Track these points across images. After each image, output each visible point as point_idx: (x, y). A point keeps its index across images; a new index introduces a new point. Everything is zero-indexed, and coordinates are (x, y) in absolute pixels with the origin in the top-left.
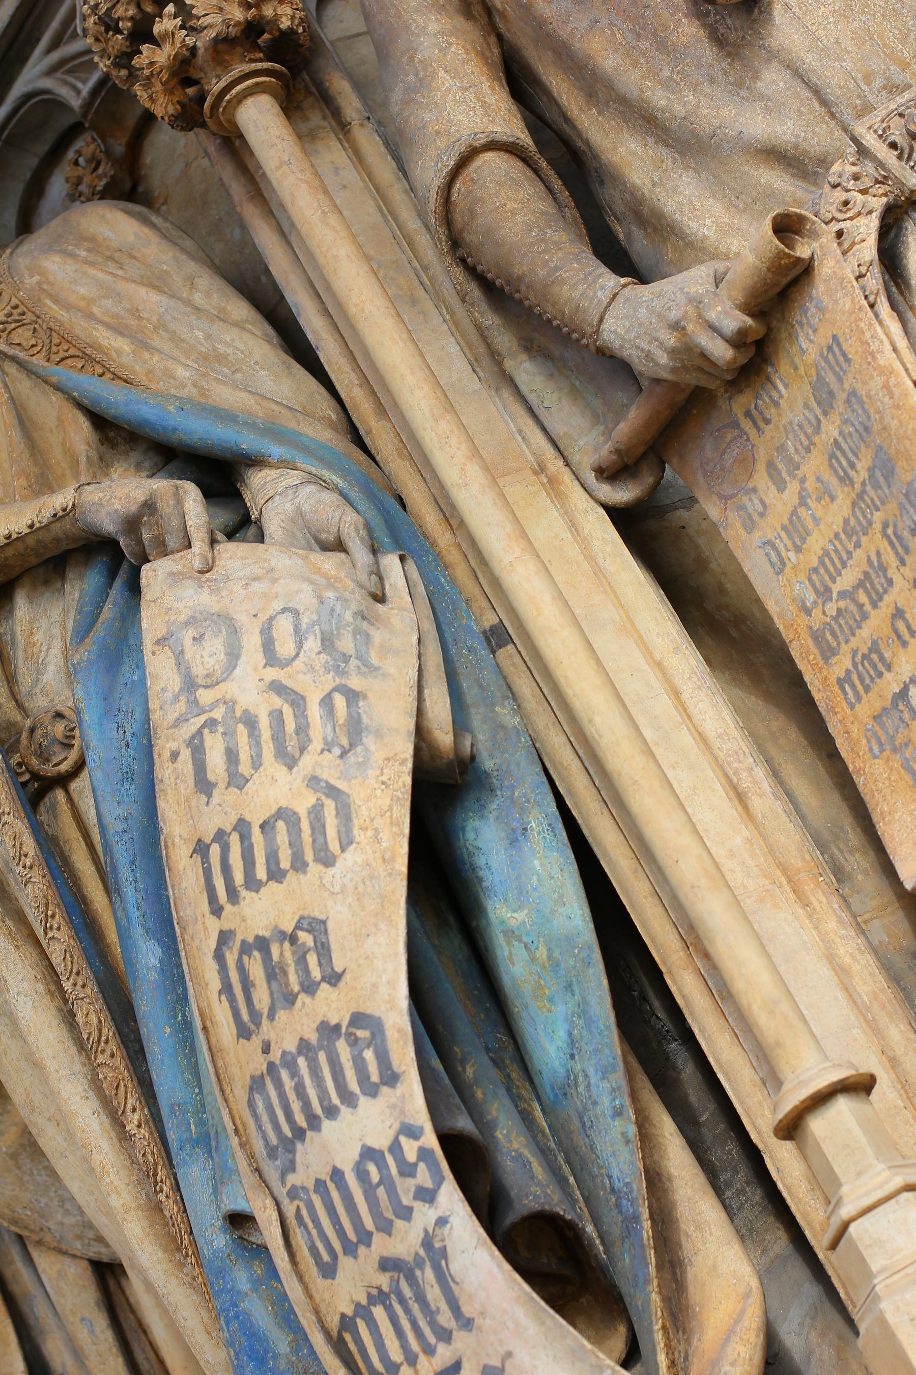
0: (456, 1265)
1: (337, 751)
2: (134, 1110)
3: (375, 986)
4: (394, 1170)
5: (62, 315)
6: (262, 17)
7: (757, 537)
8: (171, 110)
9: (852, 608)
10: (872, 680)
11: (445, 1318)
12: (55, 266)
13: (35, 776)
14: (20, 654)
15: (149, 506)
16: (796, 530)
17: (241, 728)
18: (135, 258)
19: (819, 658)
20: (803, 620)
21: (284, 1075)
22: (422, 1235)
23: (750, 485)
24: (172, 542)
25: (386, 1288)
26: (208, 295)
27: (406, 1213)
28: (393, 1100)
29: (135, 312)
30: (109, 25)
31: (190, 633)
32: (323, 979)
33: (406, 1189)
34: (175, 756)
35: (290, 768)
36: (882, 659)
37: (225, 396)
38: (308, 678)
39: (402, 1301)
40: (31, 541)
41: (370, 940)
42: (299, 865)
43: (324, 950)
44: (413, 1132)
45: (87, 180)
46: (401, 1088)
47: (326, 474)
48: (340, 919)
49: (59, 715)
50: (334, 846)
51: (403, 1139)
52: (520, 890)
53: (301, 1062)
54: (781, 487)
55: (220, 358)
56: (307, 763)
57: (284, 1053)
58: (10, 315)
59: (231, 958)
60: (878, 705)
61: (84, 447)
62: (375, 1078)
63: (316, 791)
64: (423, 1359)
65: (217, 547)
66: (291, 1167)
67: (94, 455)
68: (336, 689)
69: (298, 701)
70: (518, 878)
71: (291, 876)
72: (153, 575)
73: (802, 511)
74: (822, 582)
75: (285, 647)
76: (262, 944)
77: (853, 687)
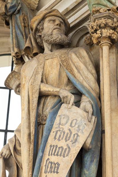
1: (72, 142)
5: (71, 63)
6: (111, 36)
8: (95, 42)
12: (74, 56)
13: (40, 122)
14: (45, 106)
15: (67, 97)
17: (63, 133)
18: (84, 58)
24: (68, 102)
26: (91, 68)
29: (80, 66)
30: (92, 28)
31: (63, 117)
34: (54, 132)
35: (66, 142)
37: (85, 84)
38: (74, 130)
40: (52, 93)
42: (60, 155)
43: (58, 168)
45: (87, 41)
47: (91, 101)
49: (46, 116)
50: (66, 155)
52: (89, 169)
55: (87, 78)
56: (68, 142)
58: (65, 60)
59: (48, 162)
61: (65, 82)
63: (67, 146)
65: (73, 106)
67: (66, 83)
68: (76, 134)
69: (71, 133)
70: (89, 167)
71: (59, 156)
72: (64, 106)
75: (73, 125)
76: (52, 163)
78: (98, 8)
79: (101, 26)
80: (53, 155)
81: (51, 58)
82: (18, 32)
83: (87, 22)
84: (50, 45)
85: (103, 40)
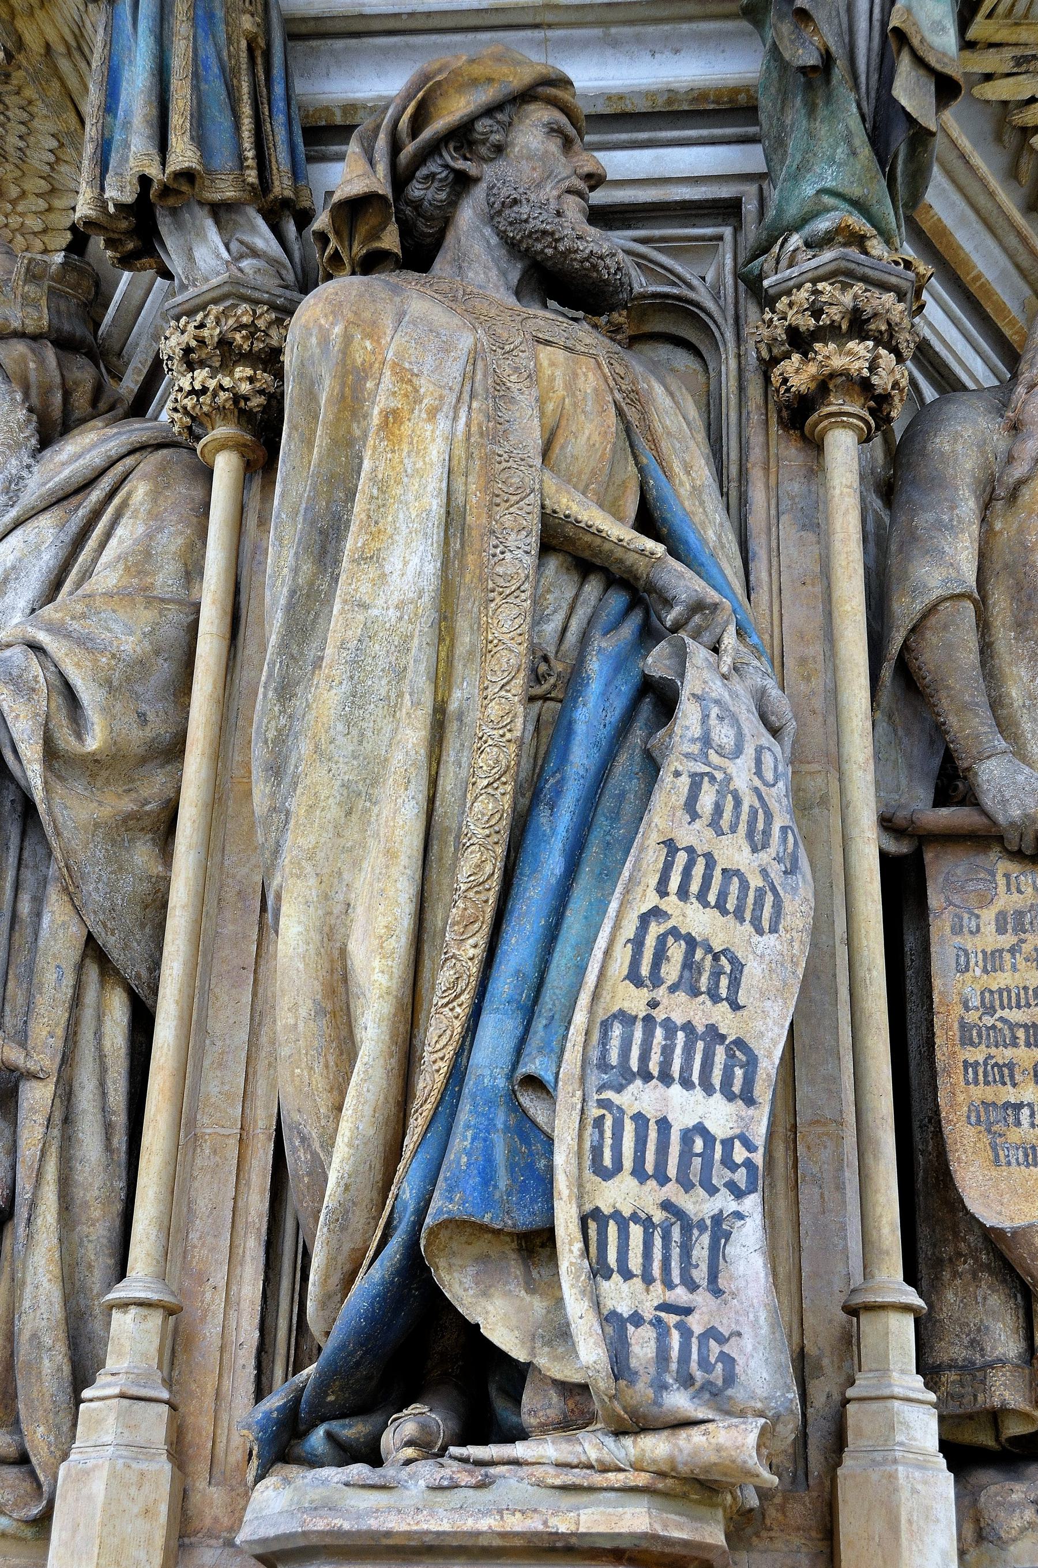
0: (732, 1250)
2: (475, 946)
3: (762, 1034)
4: (718, 1155)
7: (958, 940)
9: (1007, 1032)
10: (995, 1081)
11: (701, 1274)
12: (659, 390)
16: (993, 961)
17: (730, 797)
19: (957, 1037)
20: (959, 1010)
21: (659, 1033)
22: (716, 1211)
23: (976, 911)
25: (656, 1220)
27: (712, 1191)
28: (743, 1114)
32: (727, 999)
33: (720, 1176)
34: (677, 774)
36: (1012, 1077)
39: (666, 1238)
40: (607, 546)
41: (769, 1003)
43: (735, 983)
44: (749, 1146)
46: (751, 1111)
48: (753, 971)
51: (737, 1144)
53: (681, 1035)
54: (1001, 930)
56: (765, 857)
57: (668, 1019)
59: (655, 930)
60: (990, 1098)
62: (737, 1088)
64: (658, 1287)
66: (619, 1089)
73: (1007, 956)
74: (992, 1002)
76: (691, 943)
77: (976, 1073)
78: (857, 222)
79: (873, 327)
80: (694, 900)
81: (566, 348)
82: (208, 50)
83: (619, 233)
84: (519, 266)
85: (847, 398)
